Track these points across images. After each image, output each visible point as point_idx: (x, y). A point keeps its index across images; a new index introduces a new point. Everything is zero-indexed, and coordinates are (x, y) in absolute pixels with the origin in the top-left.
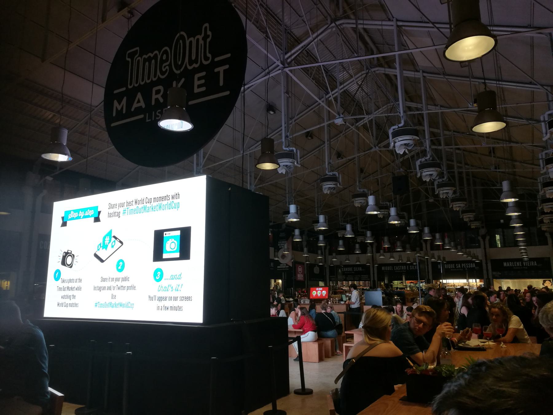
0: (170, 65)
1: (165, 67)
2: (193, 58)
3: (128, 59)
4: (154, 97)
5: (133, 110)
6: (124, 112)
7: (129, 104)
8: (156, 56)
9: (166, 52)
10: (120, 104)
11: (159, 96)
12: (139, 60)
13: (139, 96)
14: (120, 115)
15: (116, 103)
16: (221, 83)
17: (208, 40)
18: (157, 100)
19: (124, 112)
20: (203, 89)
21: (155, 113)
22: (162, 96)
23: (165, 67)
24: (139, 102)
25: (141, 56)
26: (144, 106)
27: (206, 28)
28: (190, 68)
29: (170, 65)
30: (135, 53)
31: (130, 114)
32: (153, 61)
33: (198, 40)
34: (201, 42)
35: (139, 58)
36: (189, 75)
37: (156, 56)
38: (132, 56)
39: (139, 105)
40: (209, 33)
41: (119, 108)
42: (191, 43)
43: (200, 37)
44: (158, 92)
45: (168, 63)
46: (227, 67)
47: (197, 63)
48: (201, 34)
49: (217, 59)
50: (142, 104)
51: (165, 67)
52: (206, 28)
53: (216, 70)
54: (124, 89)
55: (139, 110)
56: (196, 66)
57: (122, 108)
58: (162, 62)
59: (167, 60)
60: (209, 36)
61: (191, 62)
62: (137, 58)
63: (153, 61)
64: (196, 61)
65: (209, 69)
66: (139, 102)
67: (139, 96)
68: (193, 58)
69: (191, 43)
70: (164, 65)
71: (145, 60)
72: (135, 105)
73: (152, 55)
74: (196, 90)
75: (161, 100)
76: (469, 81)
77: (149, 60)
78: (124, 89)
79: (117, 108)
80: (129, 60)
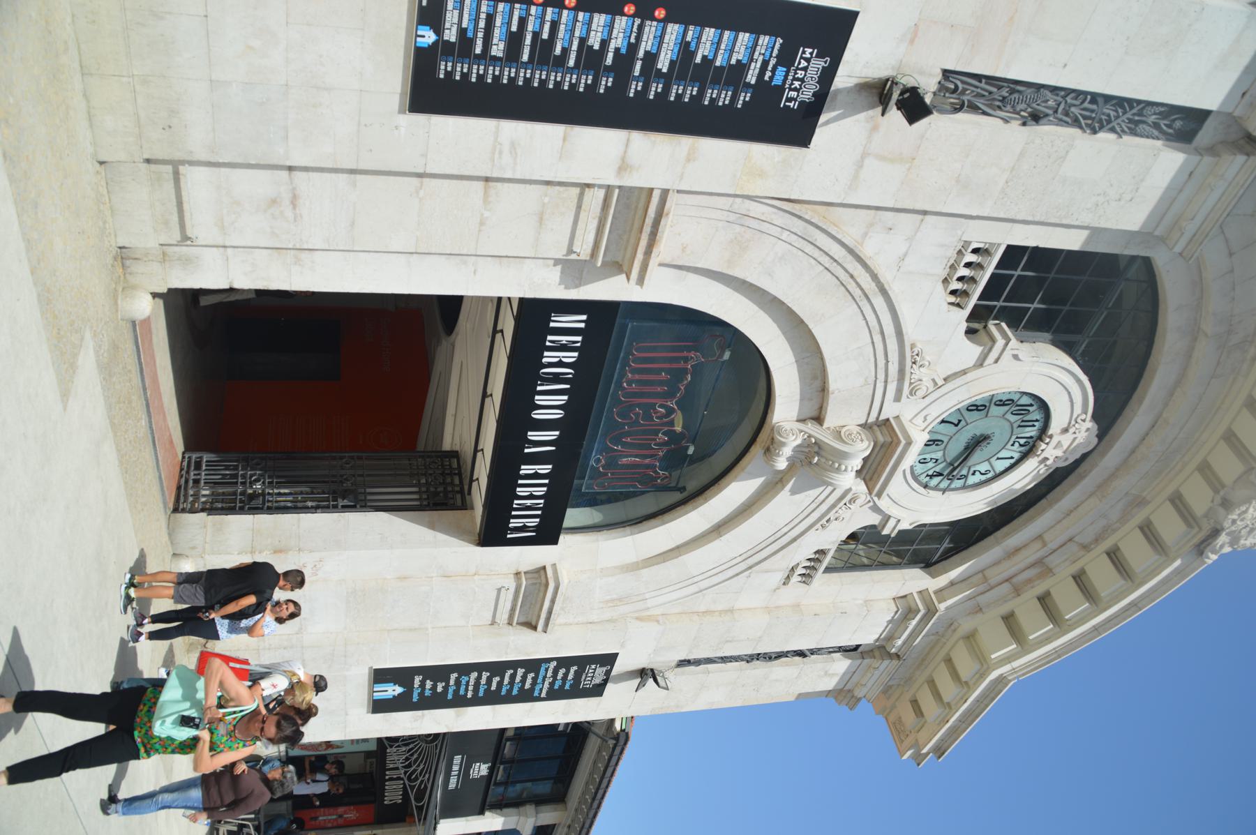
4: (799, 72)
6: (804, 56)
13: (806, 64)
14: (804, 52)
15: (811, 50)
16: (787, 104)
18: (798, 74)
19: (804, 56)
20: (789, 96)
24: (804, 64)
25: (823, 67)
26: (800, 67)
30: (826, 63)
31: (801, 58)
34: (808, 97)
38: (826, 62)
41: (807, 53)
44: (801, 74)
46: (792, 107)
49: (797, 103)
53: (793, 102)
54: (814, 55)
55: (799, 63)
62: (823, 64)
63: (815, 73)
65: (795, 100)
66: (804, 64)
67: (806, 64)
71: (818, 69)
72: (802, 61)
73: (819, 73)
74: (791, 92)
75: (796, 76)
77: (817, 71)
78: (814, 55)
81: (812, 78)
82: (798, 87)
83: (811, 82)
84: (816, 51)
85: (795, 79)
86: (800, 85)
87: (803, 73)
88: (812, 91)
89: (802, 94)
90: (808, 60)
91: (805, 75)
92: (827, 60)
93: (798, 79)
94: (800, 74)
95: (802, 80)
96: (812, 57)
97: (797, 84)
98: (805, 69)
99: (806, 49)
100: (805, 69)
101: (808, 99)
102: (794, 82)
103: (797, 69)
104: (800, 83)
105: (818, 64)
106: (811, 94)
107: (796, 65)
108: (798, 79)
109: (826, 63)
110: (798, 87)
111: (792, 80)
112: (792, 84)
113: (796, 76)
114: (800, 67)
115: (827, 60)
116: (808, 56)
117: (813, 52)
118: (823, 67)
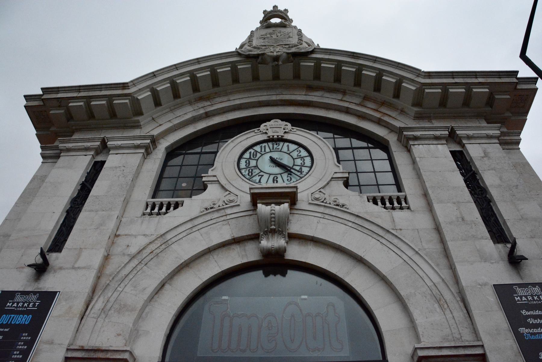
0: (530, 292)
1: (529, 292)
2: (537, 292)
4: (529, 299)
7: (521, 298)
9: (527, 289)
10: (517, 298)
11: (531, 298)
13: (523, 297)
14: (518, 301)
24: (524, 298)
28: (538, 294)
31: (522, 301)
34: (538, 290)
36: (30, 303)
37: (524, 289)
38: (516, 288)
40: (539, 288)
41: (518, 299)
43: (537, 288)
44: (530, 298)
50: (525, 299)
55: (525, 301)
57: (519, 299)
58: (527, 292)
59: (529, 291)
66: (524, 298)
67: (523, 297)
68: (537, 292)
71: (521, 290)
72: (523, 300)
73: (523, 289)
75: (532, 300)
78: (517, 295)
79: (517, 300)
82: (536, 297)
83: (530, 290)
84: (514, 295)
85: (534, 300)
86: (535, 295)
87: (528, 297)
88: (533, 288)
90: (521, 297)
91: (528, 295)
92: (515, 287)
93: (533, 298)
94: (530, 298)
95: (532, 296)
96: (518, 296)
97: (536, 298)
98: (526, 297)
100: (526, 297)
101: (539, 289)
102: (536, 299)
103: (528, 300)
104: (534, 297)
105: (519, 290)
106: (535, 289)
108: (533, 298)
110: (536, 297)
111: (535, 301)
112: (537, 300)
113: (532, 300)
115: (515, 287)
116: (519, 297)
117: (515, 296)
118: (519, 288)
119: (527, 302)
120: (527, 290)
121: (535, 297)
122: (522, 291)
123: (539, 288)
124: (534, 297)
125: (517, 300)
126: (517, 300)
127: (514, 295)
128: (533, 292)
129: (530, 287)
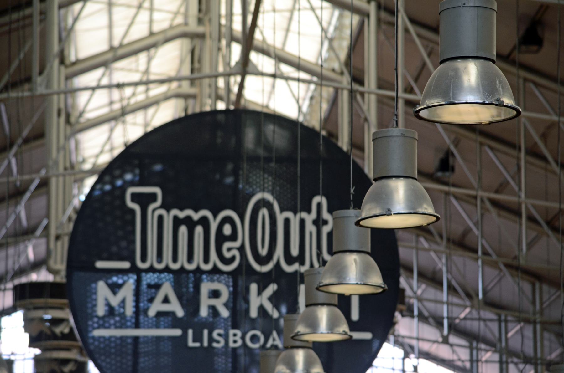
0: (241, 249)
2: (295, 252)
3: (131, 204)
5: (152, 313)
8: (204, 222)
9: (228, 220)
11: (219, 304)
12: (161, 218)
16: (355, 316)
17: (326, 229)
19: (130, 310)
21: (210, 334)
22: (226, 305)
23: (229, 250)
25: (167, 206)
26: (180, 313)
27: (319, 205)
28: (289, 269)
29: (241, 249)
30: (152, 197)
32: (199, 230)
33: (302, 222)
34: (310, 228)
35: (163, 212)
37: (204, 222)
39: (166, 308)
40: (326, 215)
41: (115, 301)
42: (287, 222)
43: (309, 218)
44: (215, 294)
45: (238, 244)
47: (302, 263)
48: (309, 211)
51: (229, 250)
52: (319, 205)
54: (126, 265)
56: (295, 267)
57: (123, 301)
58: (221, 239)
59: (233, 237)
60: (325, 222)
61: (290, 260)
63: (199, 230)
64: (301, 259)
68: (295, 252)
69: (287, 222)
70: (227, 245)
71: (177, 222)
73: (196, 216)
76: (264, 51)
77: (190, 223)
78: (126, 265)
80: (136, 207)
81: (221, 239)
82: (272, 288)
83: (244, 234)
84: (100, 264)
87: (206, 287)
88: (280, 218)
89: (301, 259)
92: (136, 197)
99: (101, 310)
101: (319, 222)
104: (254, 287)
107: (177, 332)
109: (152, 197)
110: (272, 288)
111: (253, 324)
113: (225, 313)
114: (180, 313)
115: (136, 197)
119: (177, 332)
120: (227, 230)
121: (260, 293)
122: (183, 230)
123: (326, 215)
124: (254, 287)
125: (101, 310)
126: (108, 305)
127: (100, 264)
128: (264, 252)
129: (263, 203)
